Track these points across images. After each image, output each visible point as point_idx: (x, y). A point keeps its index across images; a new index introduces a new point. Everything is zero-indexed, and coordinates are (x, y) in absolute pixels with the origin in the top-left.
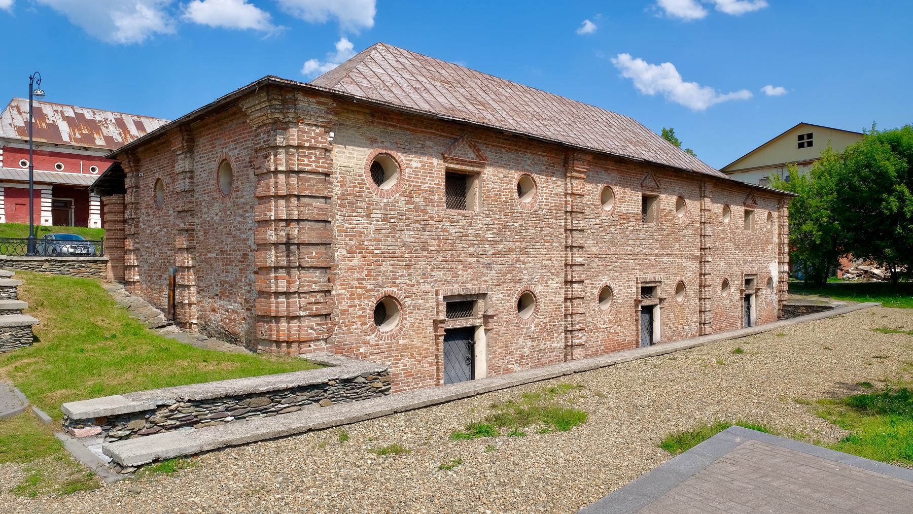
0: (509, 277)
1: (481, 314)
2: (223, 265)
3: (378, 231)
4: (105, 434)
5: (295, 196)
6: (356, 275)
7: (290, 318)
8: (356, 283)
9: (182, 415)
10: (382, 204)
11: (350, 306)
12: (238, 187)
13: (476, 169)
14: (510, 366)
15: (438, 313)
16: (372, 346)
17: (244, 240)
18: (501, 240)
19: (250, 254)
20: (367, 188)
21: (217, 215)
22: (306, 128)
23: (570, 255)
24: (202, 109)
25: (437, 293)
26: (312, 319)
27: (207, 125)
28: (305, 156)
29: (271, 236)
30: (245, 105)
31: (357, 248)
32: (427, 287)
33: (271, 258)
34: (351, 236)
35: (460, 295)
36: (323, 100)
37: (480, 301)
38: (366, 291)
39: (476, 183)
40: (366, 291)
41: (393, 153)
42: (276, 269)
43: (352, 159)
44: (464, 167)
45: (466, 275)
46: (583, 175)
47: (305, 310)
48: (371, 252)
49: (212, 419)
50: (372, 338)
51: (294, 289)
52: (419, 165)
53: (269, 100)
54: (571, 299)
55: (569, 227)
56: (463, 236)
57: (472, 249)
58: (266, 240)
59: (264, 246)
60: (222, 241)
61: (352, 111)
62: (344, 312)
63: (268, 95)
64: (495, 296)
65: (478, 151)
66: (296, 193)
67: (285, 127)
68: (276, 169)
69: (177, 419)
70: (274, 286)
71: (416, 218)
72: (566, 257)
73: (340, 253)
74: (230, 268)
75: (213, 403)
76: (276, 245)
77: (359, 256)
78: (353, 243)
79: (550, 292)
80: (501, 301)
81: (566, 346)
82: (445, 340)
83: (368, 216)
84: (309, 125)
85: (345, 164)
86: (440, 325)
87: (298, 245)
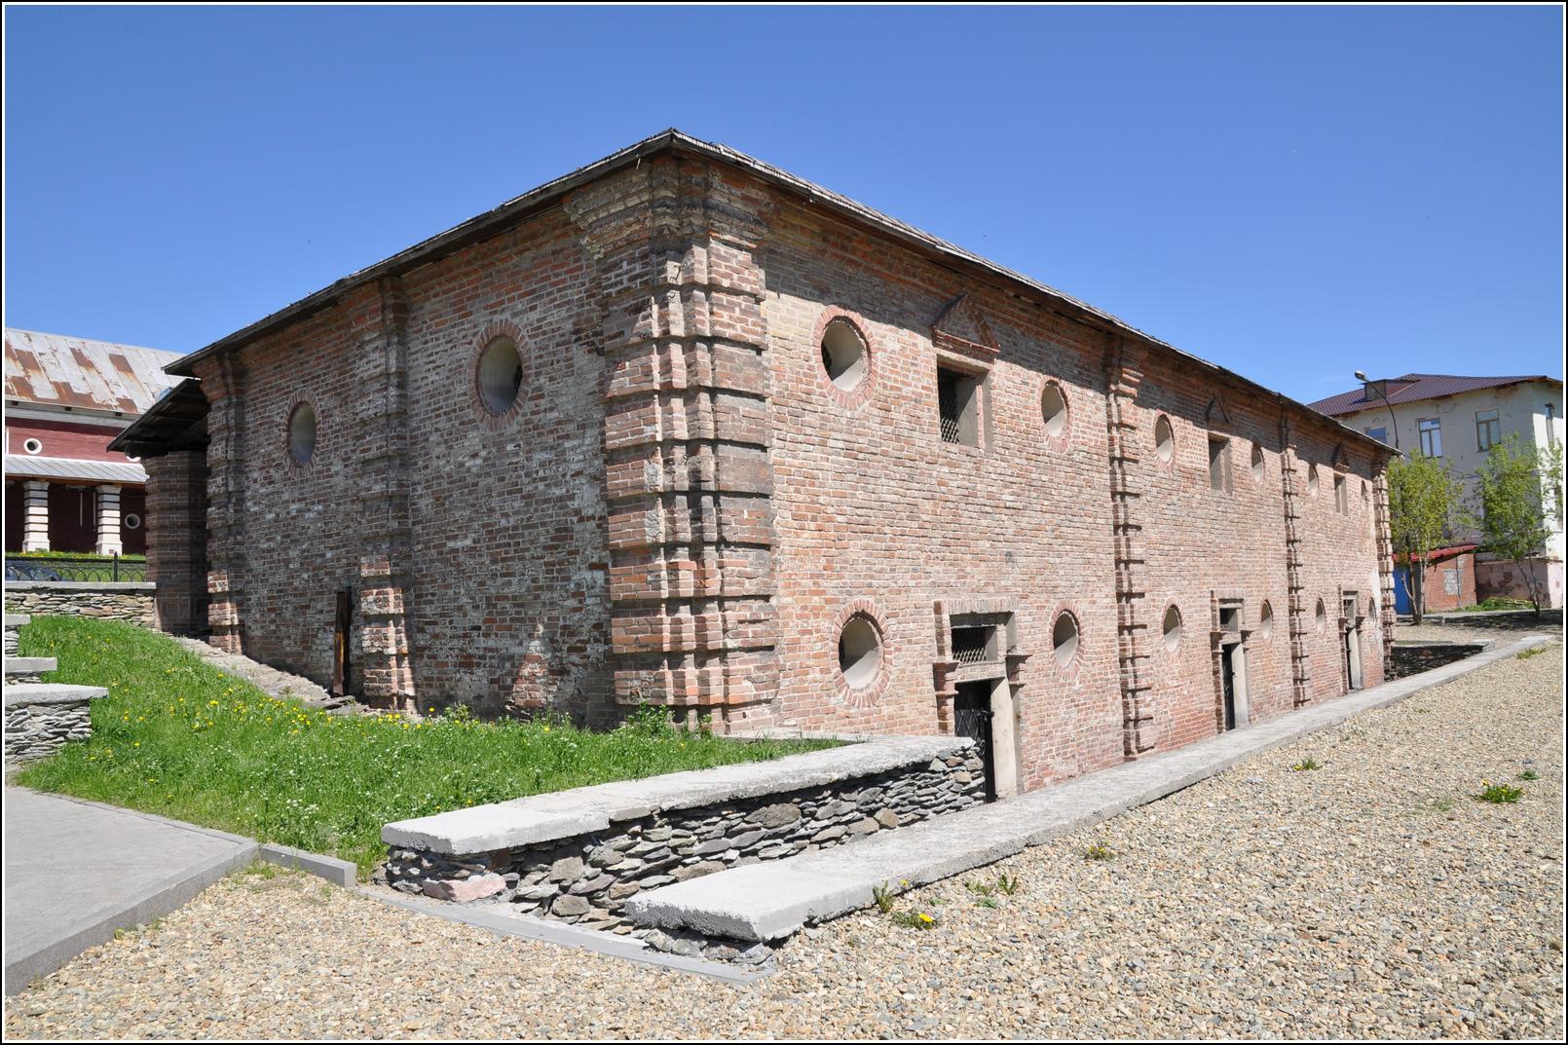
0: (1039, 580)
1: (1002, 654)
2: (494, 562)
3: (840, 475)
4: (510, 894)
5: (707, 389)
6: (808, 566)
7: (703, 655)
8: (810, 582)
9: (651, 846)
10: (844, 421)
11: (804, 632)
12: (539, 389)
13: (981, 364)
14: (1049, 761)
15: (941, 651)
16: (840, 718)
17: (561, 499)
18: (1025, 508)
19: (577, 527)
20: (820, 386)
21: (475, 456)
22: (723, 249)
23: (1123, 542)
24: (461, 229)
25: (938, 608)
26: (746, 656)
27: (450, 270)
28: (724, 307)
29: (655, 474)
30: (574, 211)
31: (808, 509)
32: (919, 595)
33: (656, 524)
34: (799, 483)
35: (973, 615)
36: (753, 193)
37: (1001, 628)
38: (828, 601)
39: (979, 390)
40: (828, 601)
41: (855, 316)
42: (671, 548)
43: (796, 321)
44: (963, 358)
45: (977, 574)
46: (1133, 391)
47: (737, 635)
48: (830, 520)
49: (704, 856)
50: (837, 701)
51: (713, 588)
52: (897, 347)
53: (652, 189)
54: (1130, 629)
55: (1120, 488)
56: (969, 495)
57: (984, 522)
58: (641, 486)
59: (641, 500)
60: (492, 510)
61: (793, 226)
62: (794, 645)
63: (650, 178)
64: (1022, 618)
65: (985, 327)
66: (709, 384)
67: (681, 251)
68: (666, 332)
69: (641, 855)
70: (665, 584)
71: (897, 454)
72: (1118, 546)
73: (783, 518)
74: (517, 566)
75: (702, 818)
76: (668, 497)
77: (813, 525)
78: (801, 497)
79: (1097, 614)
80: (1031, 632)
81: (1127, 721)
82: (957, 707)
83: (823, 444)
84: (727, 243)
85: (782, 334)
86: (949, 676)
87: (716, 495)
